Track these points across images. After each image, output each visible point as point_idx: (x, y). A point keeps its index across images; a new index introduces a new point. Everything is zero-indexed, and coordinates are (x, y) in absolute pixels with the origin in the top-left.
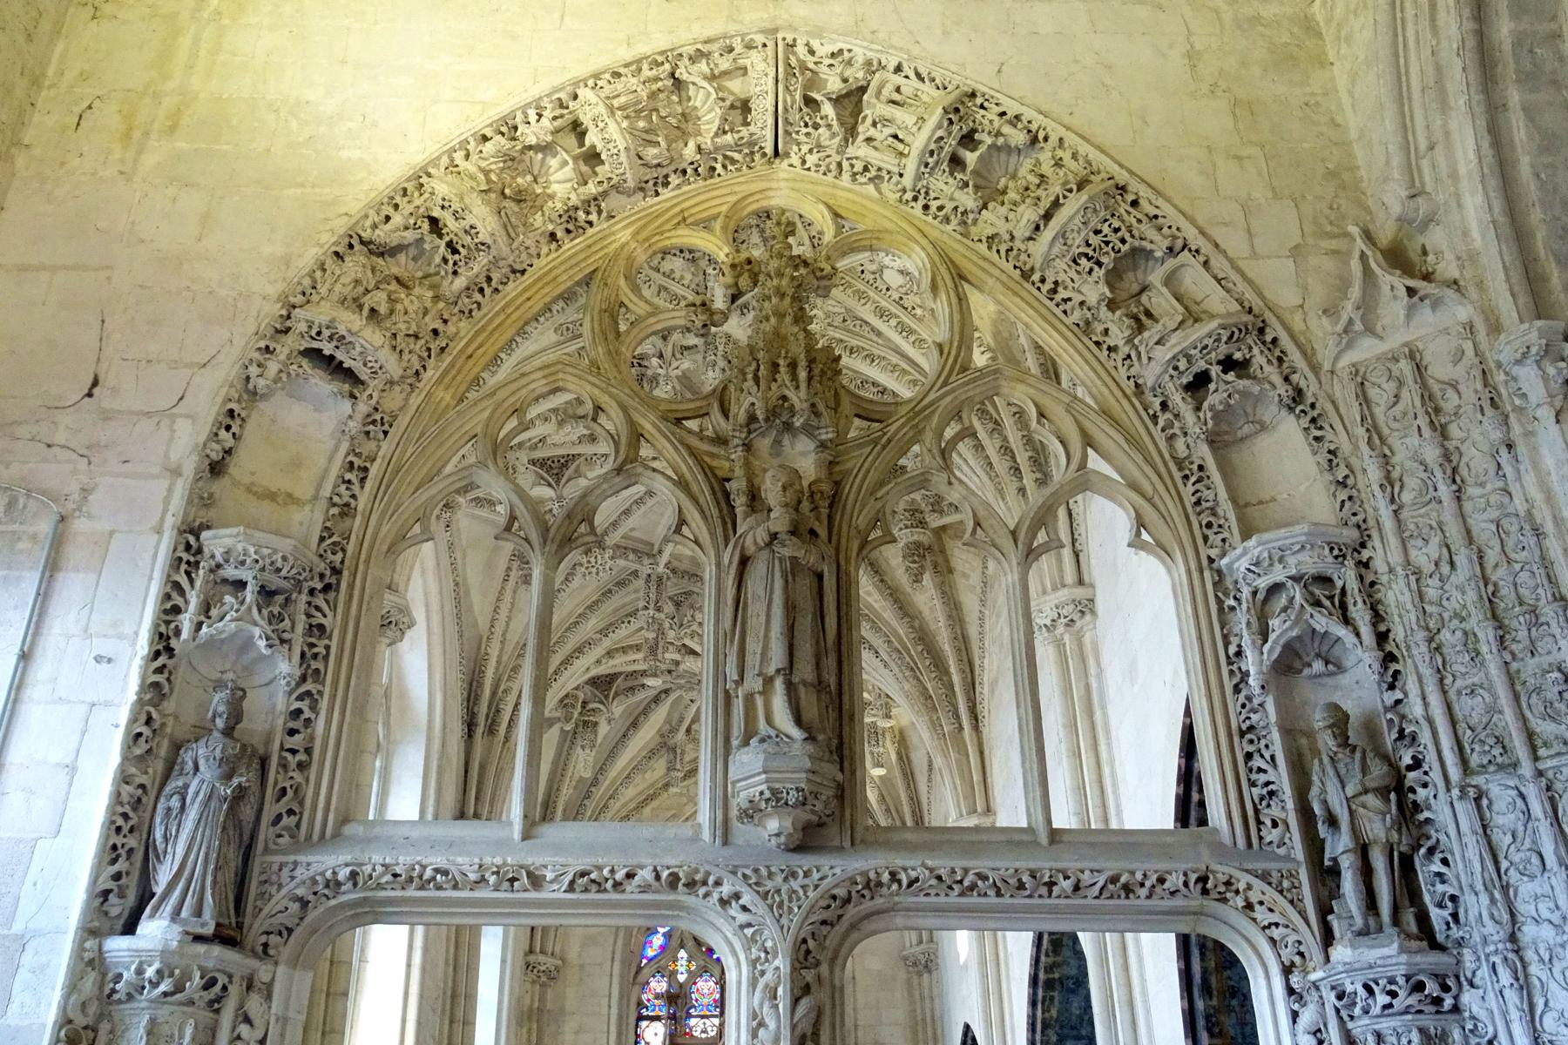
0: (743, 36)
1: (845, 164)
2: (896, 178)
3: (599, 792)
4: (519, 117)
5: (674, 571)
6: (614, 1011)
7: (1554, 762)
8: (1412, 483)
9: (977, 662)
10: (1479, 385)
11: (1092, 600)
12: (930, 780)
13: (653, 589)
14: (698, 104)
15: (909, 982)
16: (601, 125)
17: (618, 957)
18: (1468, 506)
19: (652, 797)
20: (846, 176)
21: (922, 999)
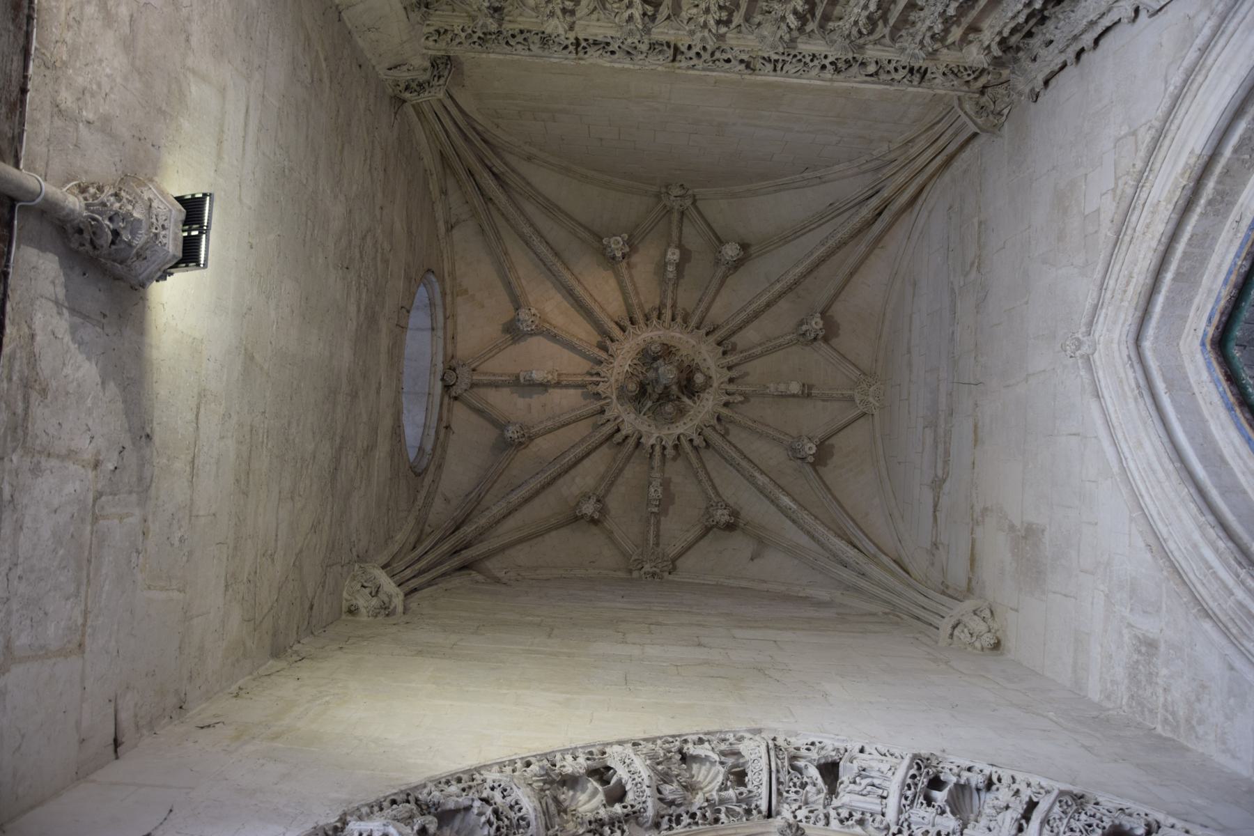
0: (735, 733)
1: (833, 814)
2: (879, 818)
4: (559, 756)
14: (701, 778)
16: (628, 761)
20: (834, 823)
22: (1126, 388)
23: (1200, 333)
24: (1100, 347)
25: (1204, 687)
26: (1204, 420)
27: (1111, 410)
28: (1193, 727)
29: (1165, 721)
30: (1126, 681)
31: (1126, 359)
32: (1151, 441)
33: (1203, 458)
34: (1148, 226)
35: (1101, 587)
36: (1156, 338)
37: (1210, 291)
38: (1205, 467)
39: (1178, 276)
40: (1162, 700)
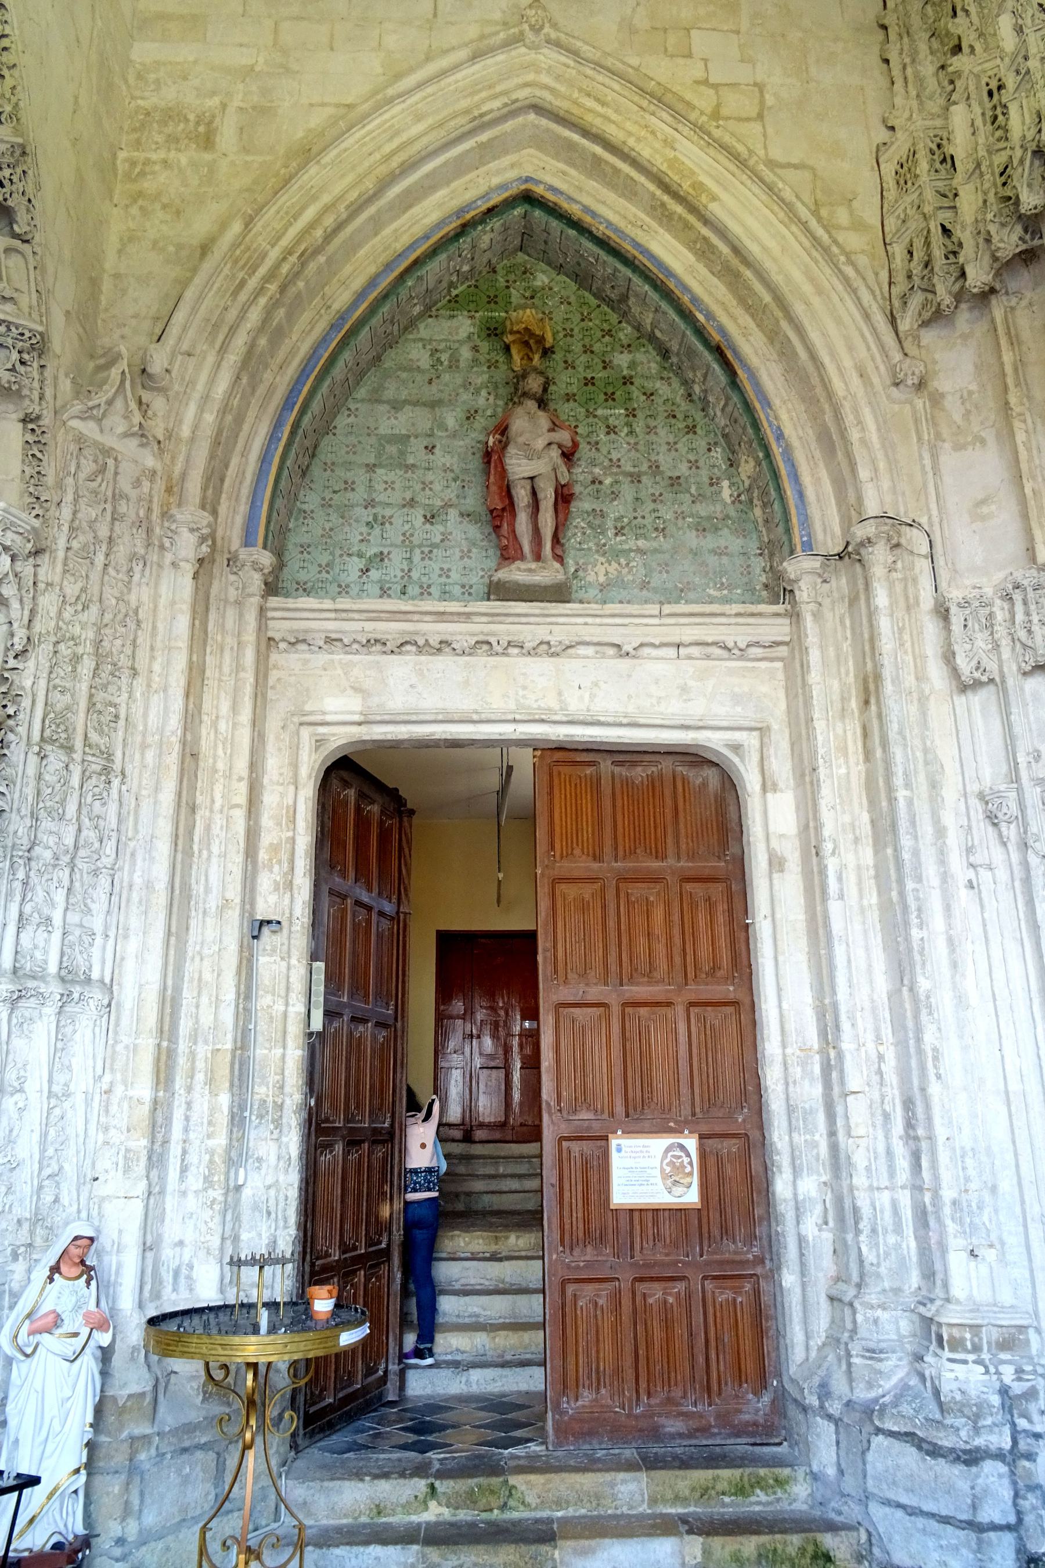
7: (93, 759)
8: (82, 538)
10: (142, 513)
18: (106, 578)
22: (484, 94)
23: (540, 175)
24: (532, 55)
25: (178, 213)
26: (448, 183)
27: (459, 76)
28: (135, 201)
29: (133, 163)
30: (163, 104)
31: (514, 97)
32: (425, 133)
33: (407, 191)
34: (653, 133)
35: (261, 60)
36: (537, 127)
37: (580, 189)
38: (398, 196)
39: (597, 160)
40: (154, 157)
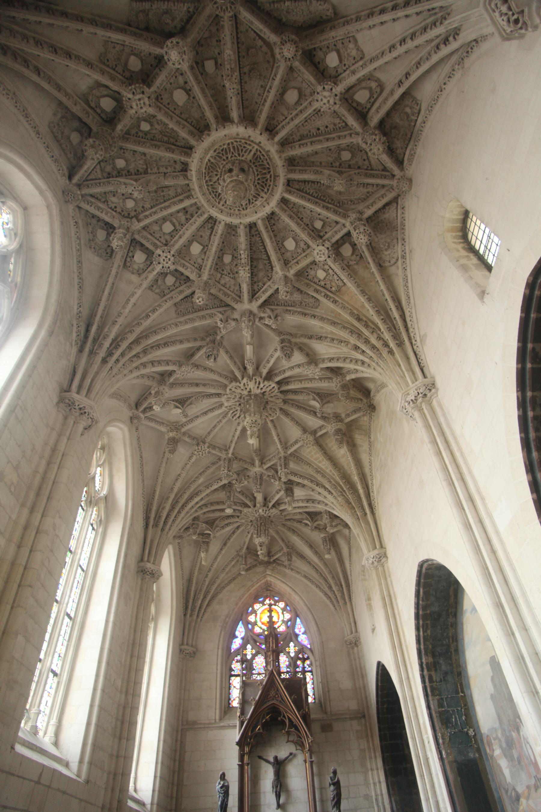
3: (210, 575)
5: (236, 458)
6: (219, 671)
9: (370, 482)
11: (434, 384)
12: (350, 561)
13: (227, 462)
15: (348, 652)
17: (220, 647)
19: (234, 579)
21: (355, 659)
